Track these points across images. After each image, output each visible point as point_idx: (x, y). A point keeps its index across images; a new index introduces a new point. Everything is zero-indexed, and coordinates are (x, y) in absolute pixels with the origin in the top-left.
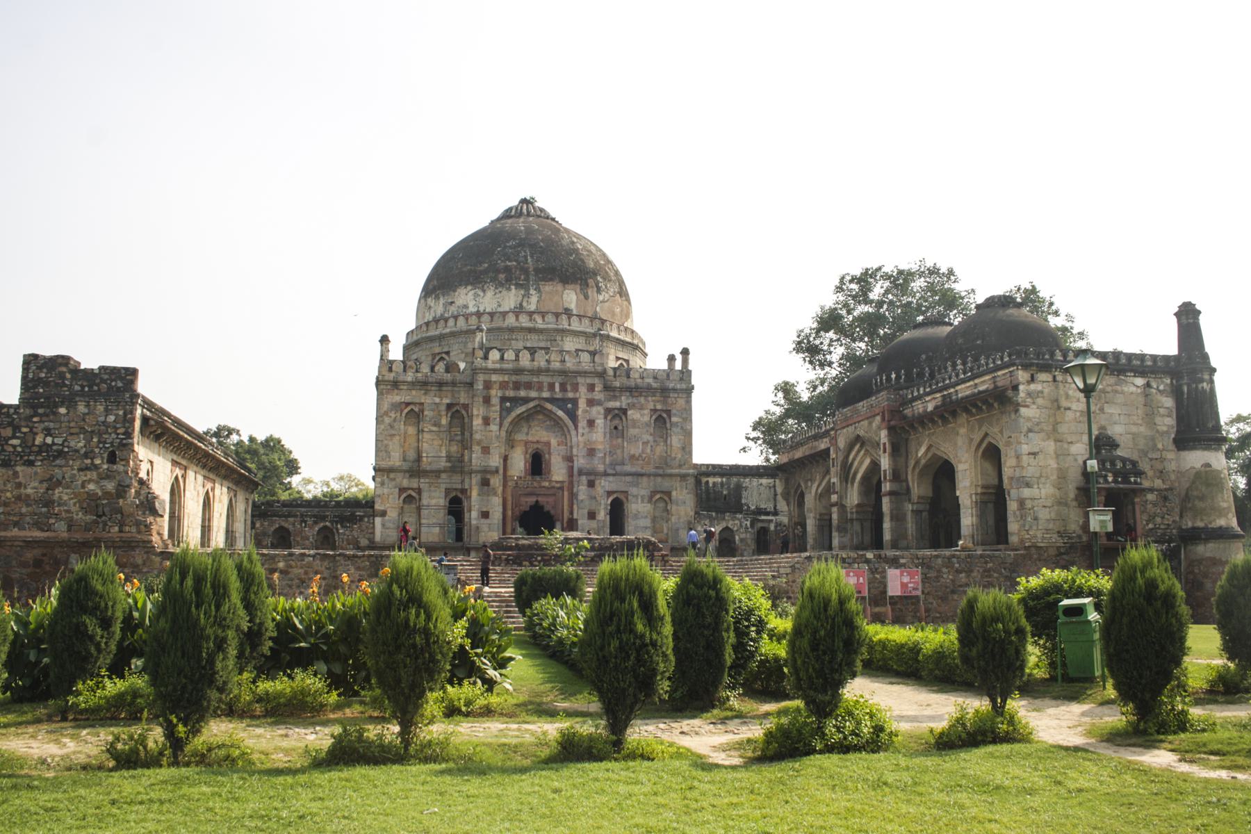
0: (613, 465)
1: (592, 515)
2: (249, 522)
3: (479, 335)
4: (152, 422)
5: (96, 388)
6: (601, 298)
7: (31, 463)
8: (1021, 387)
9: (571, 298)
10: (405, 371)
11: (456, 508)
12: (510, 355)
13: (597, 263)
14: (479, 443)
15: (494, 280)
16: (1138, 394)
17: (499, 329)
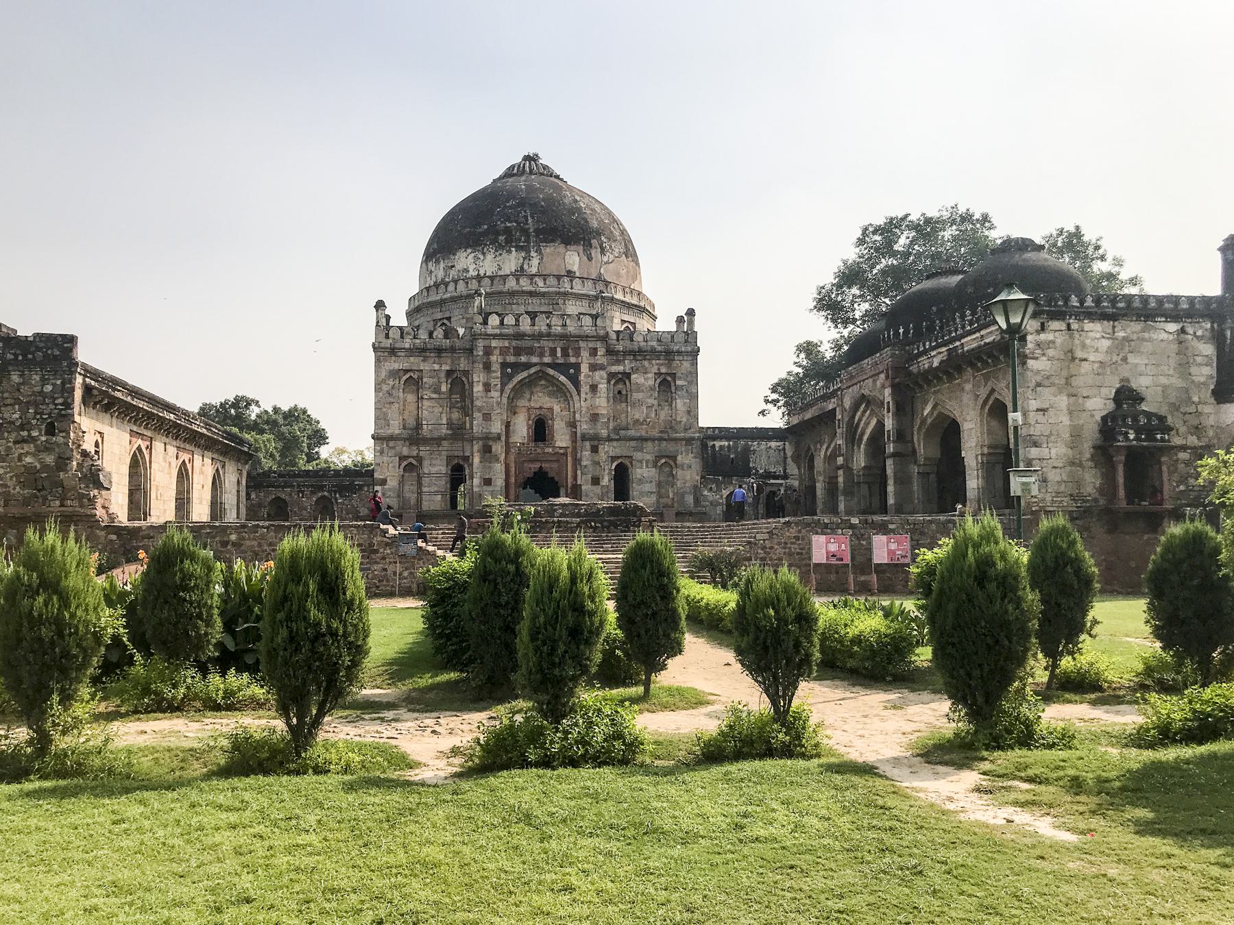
0: (617, 430)
1: (596, 481)
2: (243, 494)
3: (477, 301)
4: (95, 392)
5: (30, 356)
6: (605, 259)
8: (1029, 338)
9: (573, 259)
10: (402, 337)
11: (457, 475)
12: (510, 320)
13: (601, 222)
14: (479, 411)
16: (1169, 342)
17: (500, 293)
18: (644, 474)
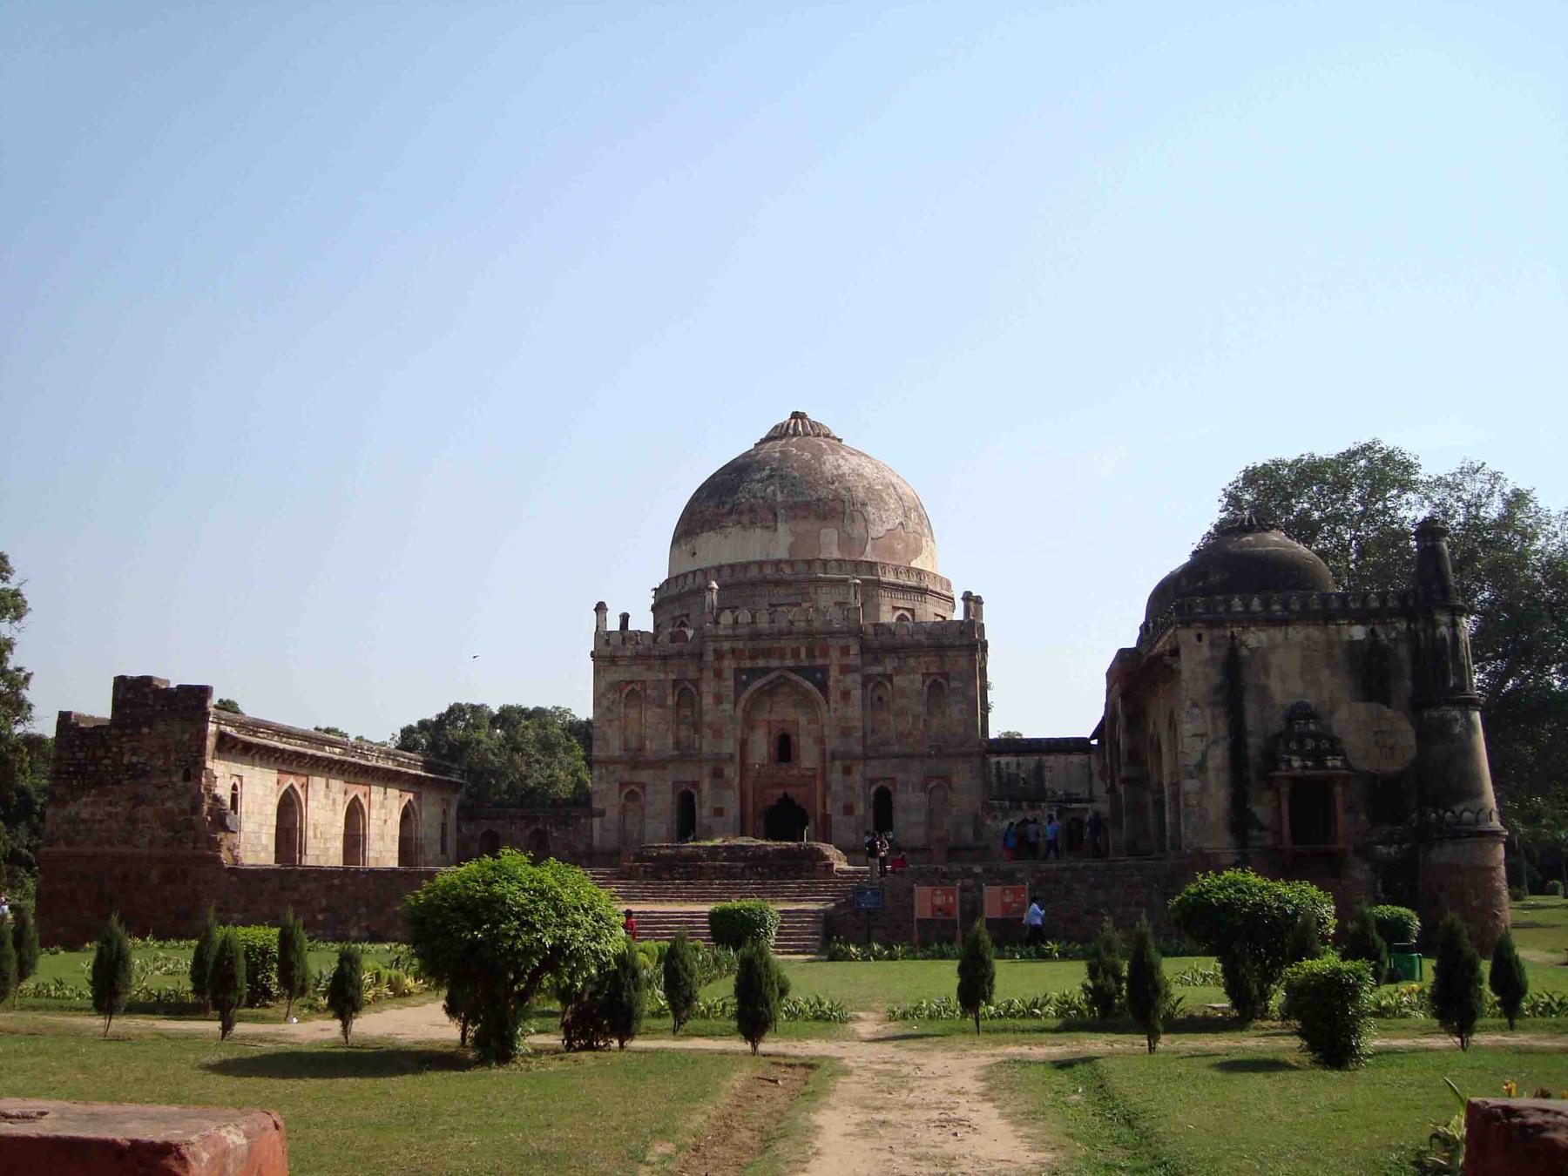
1: (848, 810)
7: (119, 782)
17: (739, 584)
18: (910, 802)
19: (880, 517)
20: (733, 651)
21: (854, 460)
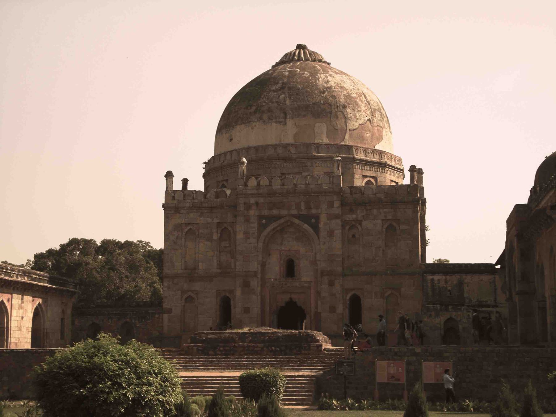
1: (333, 309)
2: (68, 322)
10: (184, 199)
13: (348, 97)
15: (261, 118)
18: (372, 303)
19: (355, 116)
20: (257, 204)
21: (338, 78)
